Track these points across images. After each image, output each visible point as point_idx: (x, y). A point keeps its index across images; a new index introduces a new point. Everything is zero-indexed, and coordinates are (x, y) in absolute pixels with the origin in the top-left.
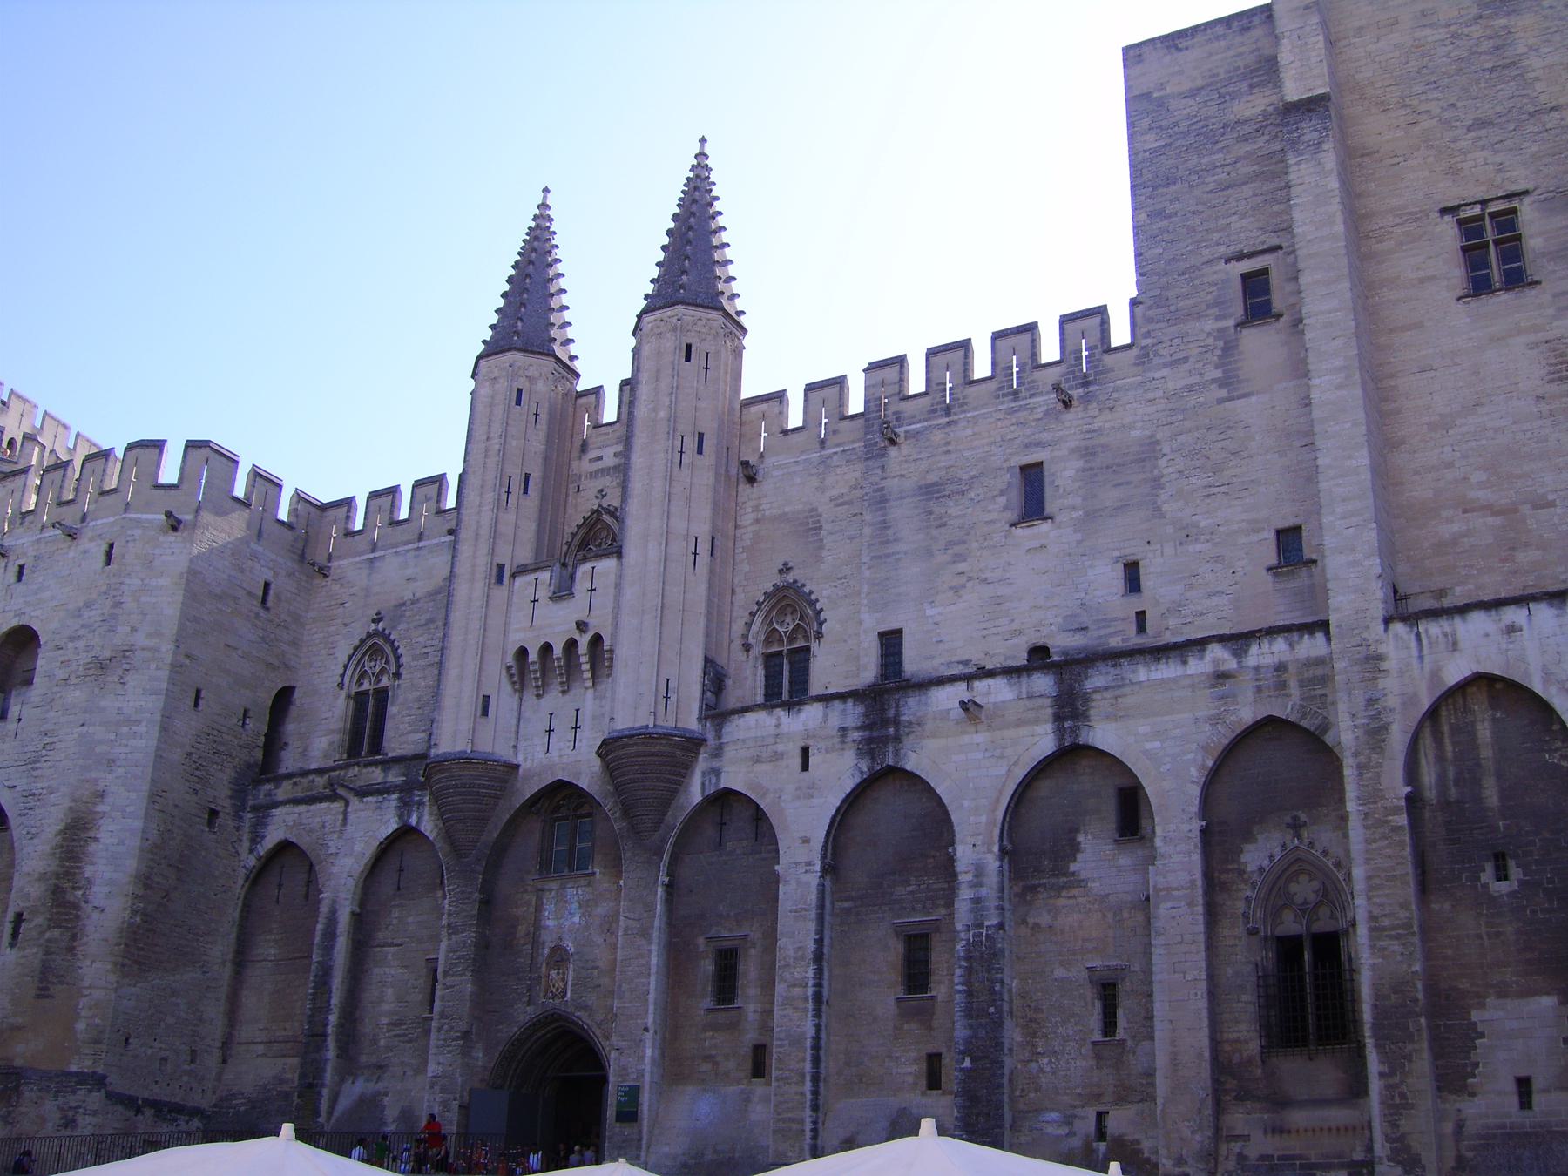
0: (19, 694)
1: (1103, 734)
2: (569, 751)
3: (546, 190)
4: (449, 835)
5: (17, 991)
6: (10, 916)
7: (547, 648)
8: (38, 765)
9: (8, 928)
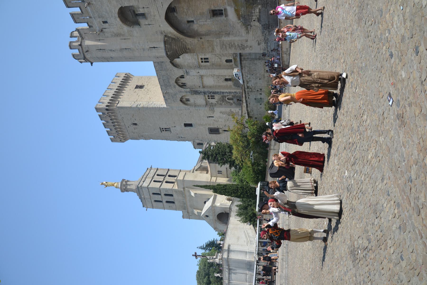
0: (137, 10)
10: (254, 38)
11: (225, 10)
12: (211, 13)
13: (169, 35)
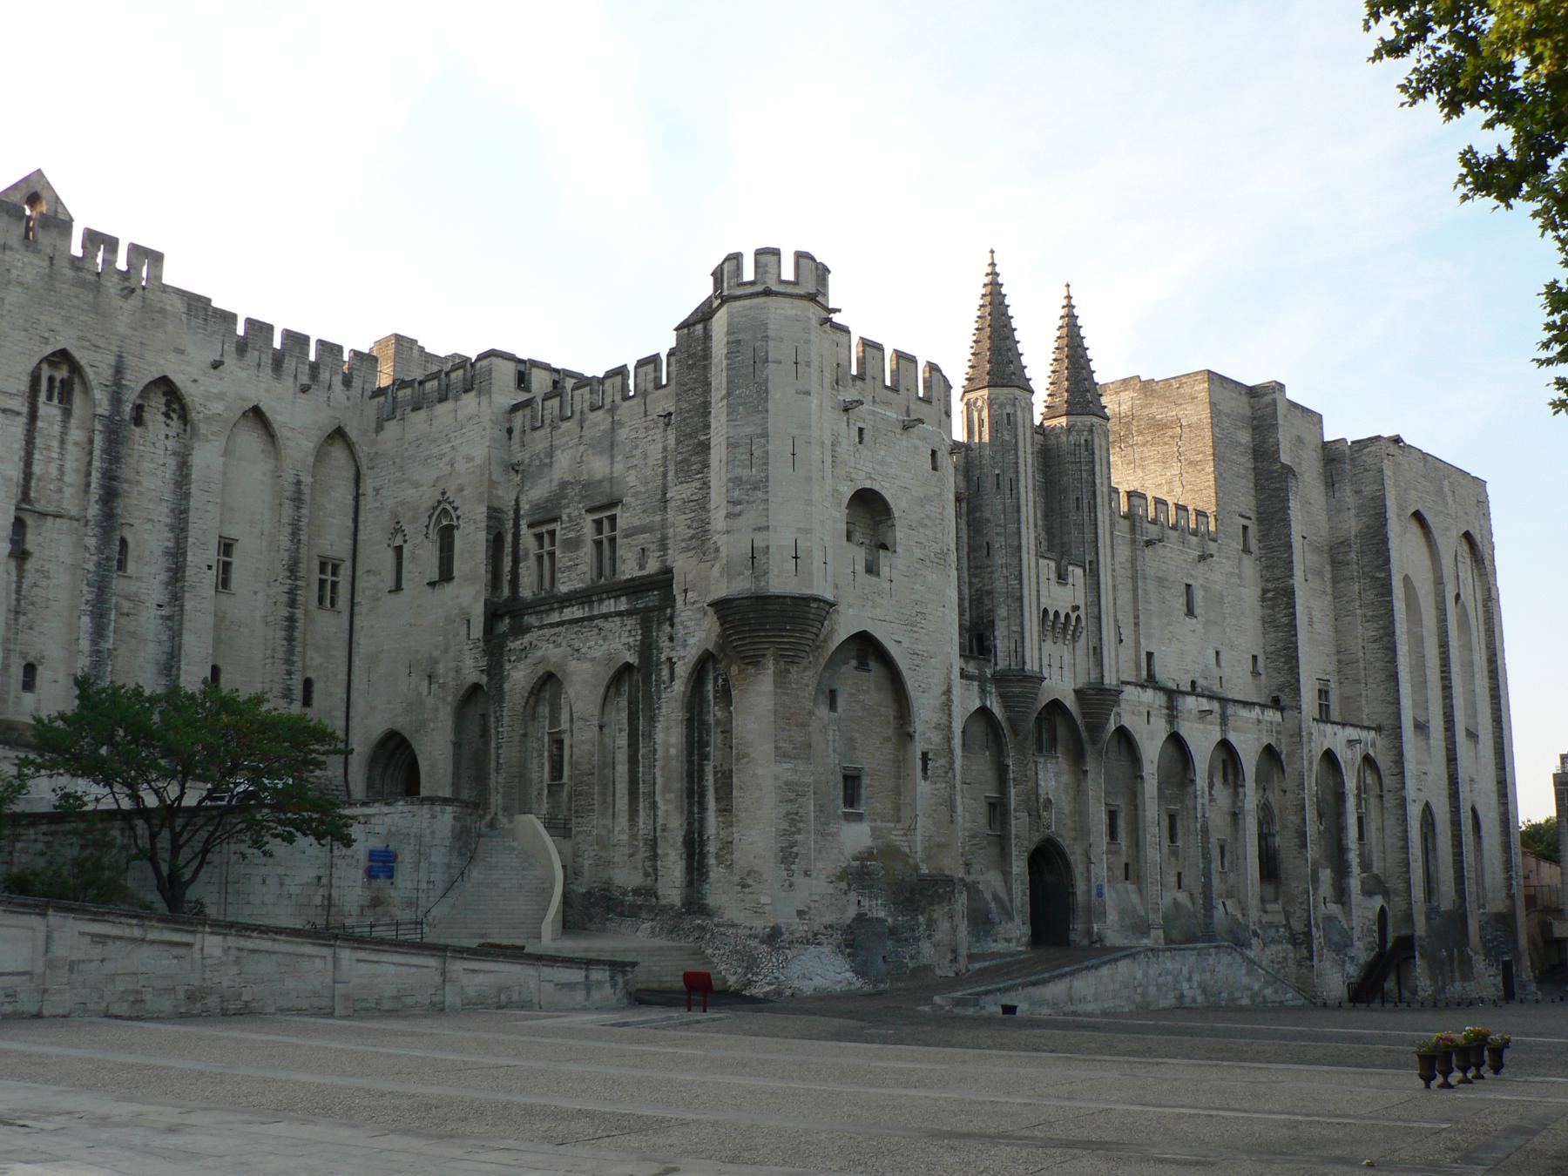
1: (1233, 738)
2: (1059, 682)
3: (992, 252)
4: (1009, 719)
5: (935, 815)
6: (919, 755)
7: (1056, 613)
8: (915, 629)
9: (919, 764)
10: (817, 898)
11: (859, 817)
12: (854, 773)
13: (826, 623)
